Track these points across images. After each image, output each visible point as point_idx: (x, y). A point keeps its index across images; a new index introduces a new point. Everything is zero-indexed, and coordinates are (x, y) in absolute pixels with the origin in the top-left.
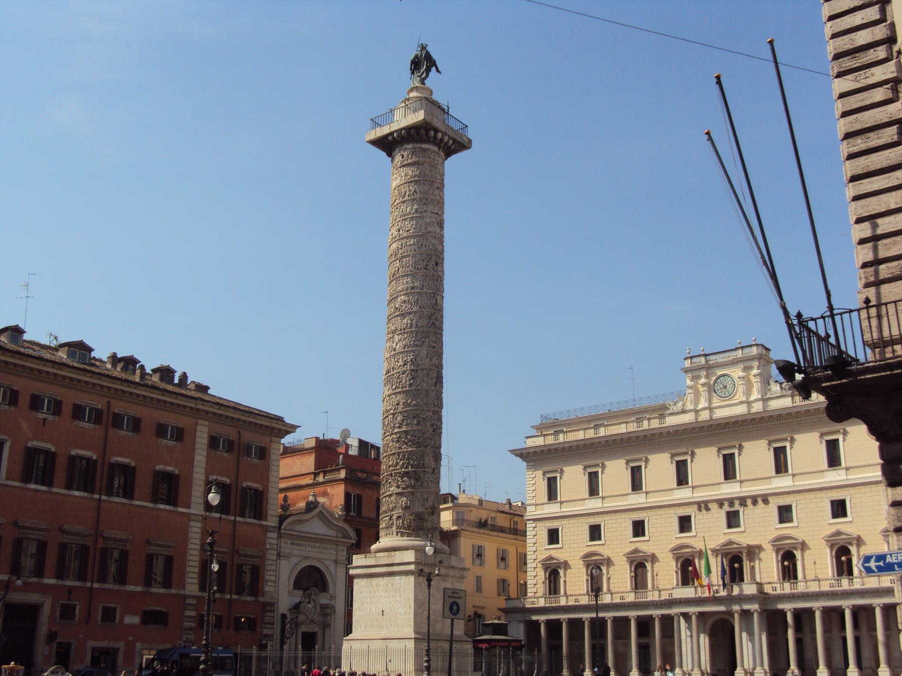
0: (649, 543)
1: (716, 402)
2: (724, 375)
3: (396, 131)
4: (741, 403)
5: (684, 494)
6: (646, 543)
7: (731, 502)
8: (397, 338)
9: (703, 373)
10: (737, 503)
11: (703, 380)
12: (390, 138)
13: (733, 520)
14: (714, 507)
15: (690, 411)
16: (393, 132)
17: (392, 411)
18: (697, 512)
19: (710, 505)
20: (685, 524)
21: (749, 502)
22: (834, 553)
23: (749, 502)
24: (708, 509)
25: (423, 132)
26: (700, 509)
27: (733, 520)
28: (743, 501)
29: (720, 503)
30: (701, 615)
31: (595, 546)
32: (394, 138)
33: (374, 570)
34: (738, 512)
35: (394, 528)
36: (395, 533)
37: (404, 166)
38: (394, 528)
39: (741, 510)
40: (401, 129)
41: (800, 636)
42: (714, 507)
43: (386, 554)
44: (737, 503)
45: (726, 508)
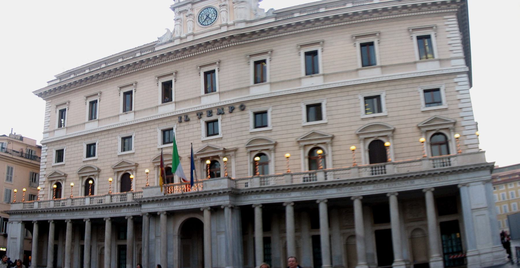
0: (135, 155)
1: (198, 29)
4: (221, 26)
5: (169, 109)
6: (132, 156)
7: (210, 113)
9: (190, 6)
10: (215, 111)
13: (211, 128)
14: (193, 118)
18: (178, 125)
19: (189, 116)
20: (167, 135)
24: (187, 120)
26: (180, 122)
27: (211, 128)
28: (221, 112)
29: (200, 115)
31: (91, 162)
39: (220, 118)
41: (267, 235)
42: (193, 118)
44: (215, 111)
45: (205, 118)
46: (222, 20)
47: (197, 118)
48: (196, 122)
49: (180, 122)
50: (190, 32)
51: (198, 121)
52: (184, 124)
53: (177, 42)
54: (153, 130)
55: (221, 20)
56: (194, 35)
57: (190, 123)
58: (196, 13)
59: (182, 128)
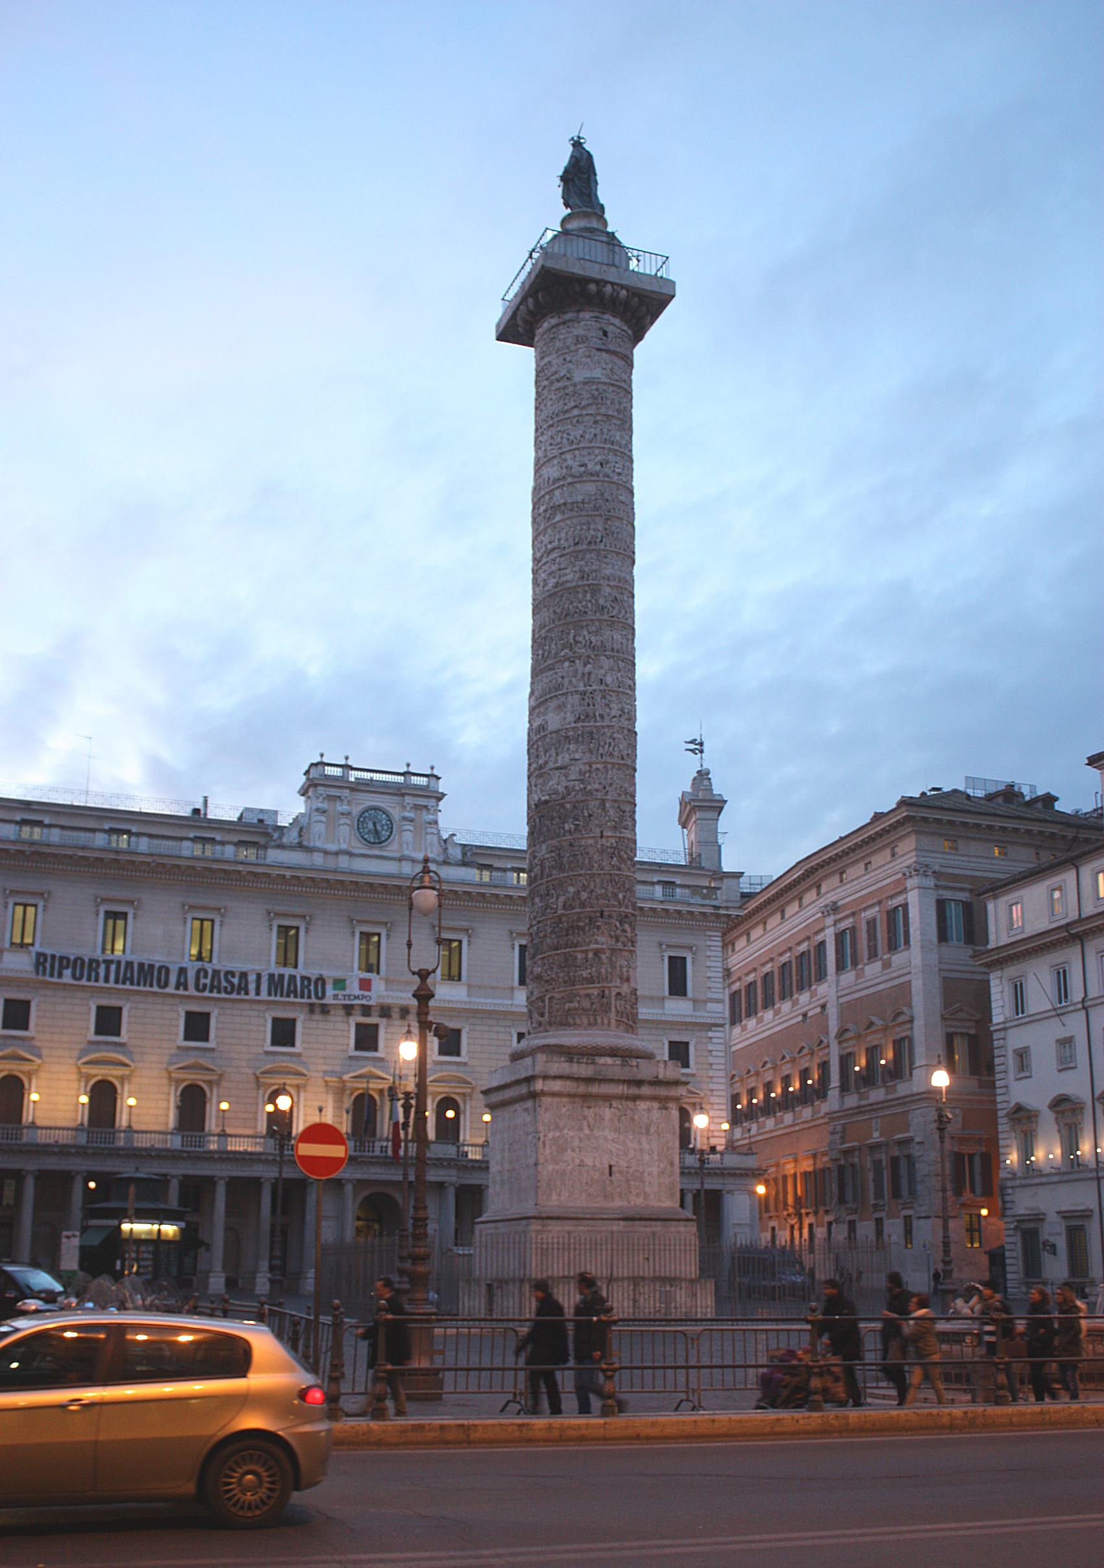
0: (216, 1054)
1: (359, 847)
2: (376, 809)
3: (612, 284)
6: (208, 1054)
7: (366, 1010)
8: (606, 663)
9: (346, 792)
10: (375, 1012)
11: (345, 808)
12: (592, 287)
15: (318, 850)
16: (607, 282)
17: (600, 795)
18: (308, 1017)
21: (396, 1014)
22: (178, 1093)
23: (396, 1014)
25: (644, 309)
28: (385, 1011)
29: (348, 1010)
30: (360, 1184)
32: (599, 293)
33: (595, 1089)
34: (376, 1026)
35: (613, 1015)
36: (613, 1022)
37: (607, 351)
38: (613, 1015)
39: (383, 1022)
40: (623, 287)
43: (618, 1061)
44: (375, 1012)
46: (405, 846)
47: (342, 1012)
48: (340, 1019)
49: (312, 1011)
50: (344, 846)
51: (345, 1019)
52: (318, 1017)
53: (318, 859)
54: (256, 1013)
55: (401, 845)
56: (350, 854)
57: (329, 1018)
58: (356, 810)
59: (313, 1024)
